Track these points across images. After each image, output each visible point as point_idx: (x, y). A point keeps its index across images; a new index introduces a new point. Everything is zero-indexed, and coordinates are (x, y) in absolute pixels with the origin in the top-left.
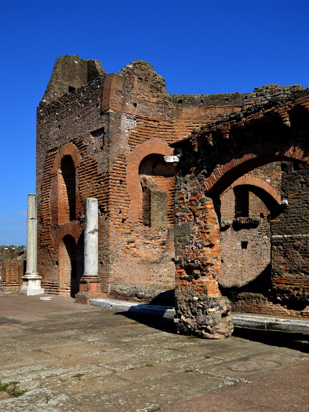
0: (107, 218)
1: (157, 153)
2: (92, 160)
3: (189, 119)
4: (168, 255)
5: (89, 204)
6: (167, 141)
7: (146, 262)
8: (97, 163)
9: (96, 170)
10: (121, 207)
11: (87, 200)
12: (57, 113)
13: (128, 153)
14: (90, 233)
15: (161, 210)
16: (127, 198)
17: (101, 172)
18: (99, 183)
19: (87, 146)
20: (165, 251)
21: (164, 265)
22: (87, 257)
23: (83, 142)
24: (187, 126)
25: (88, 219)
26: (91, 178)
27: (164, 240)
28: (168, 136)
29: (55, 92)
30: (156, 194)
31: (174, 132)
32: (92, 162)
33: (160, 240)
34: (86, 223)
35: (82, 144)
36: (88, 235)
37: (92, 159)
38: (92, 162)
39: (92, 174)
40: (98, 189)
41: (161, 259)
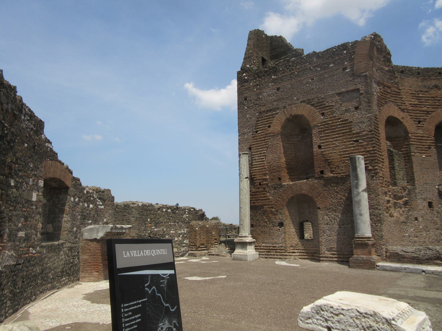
0: (373, 176)
1: (393, 115)
2: (341, 120)
3: (411, 87)
4: (412, 214)
5: (359, 162)
6: (398, 105)
7: (397, 222)
8: (351, 122)
9: (351, 128)
10: (380, 165)
11: (357, 159)
12: (273, 77)
13: (377, 113)
14: (363, 191)
15: (401, 170)
16: (383, 157)
17: (358, 131)
18: (356, 141)
19: (332, 106)
20: (409, 210)
21: (410, 225)
22: (363, 216)
23: (325, 102)
24: (411, 94)
25: (360, 177)
26: (343, 136)
27: (406, 199)
28: (398, 101)
29: (254, 59)
30: (396, 154)
31: (402, 98)
32: (341, 121)
33: (404, 199)
34: (358, 181)
35: (325, 104)
36: (362, 193)
37: (342, 119)
38: (341, 121)
39: (343, 132)
40: (353, 147)
41: (407, 218)
